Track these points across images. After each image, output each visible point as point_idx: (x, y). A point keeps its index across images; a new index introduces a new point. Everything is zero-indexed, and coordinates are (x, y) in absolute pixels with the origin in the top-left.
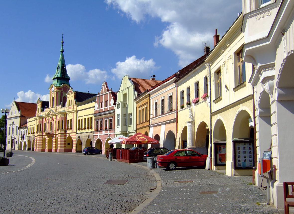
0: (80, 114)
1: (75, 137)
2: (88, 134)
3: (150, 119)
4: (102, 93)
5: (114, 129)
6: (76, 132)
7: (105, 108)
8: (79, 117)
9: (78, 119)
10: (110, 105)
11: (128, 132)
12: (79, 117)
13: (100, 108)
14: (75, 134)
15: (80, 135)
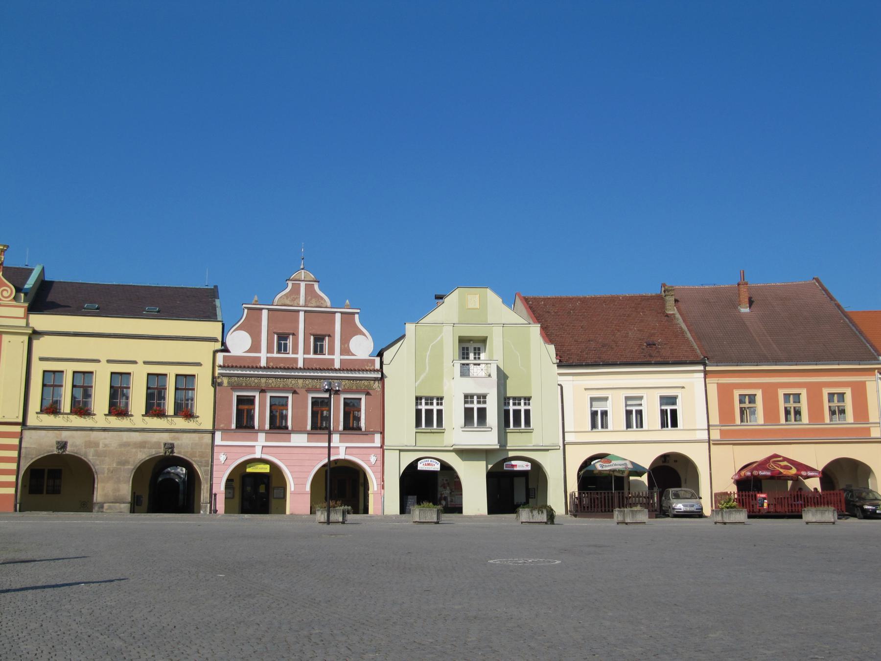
0: (41, 346)
1: (16, 441)
2: (166, 438)
3: (709, 426)
4: (288, 302)
5: (382, 433)
6: (20, 420)
7: (312, 356)
8: (41, 359)
9: (38, 369)
10: (345, 350)
11: (508, 448)
12: (41, 359)
13: (270, 350)
14: (18, 429)
15: (64, 435)
